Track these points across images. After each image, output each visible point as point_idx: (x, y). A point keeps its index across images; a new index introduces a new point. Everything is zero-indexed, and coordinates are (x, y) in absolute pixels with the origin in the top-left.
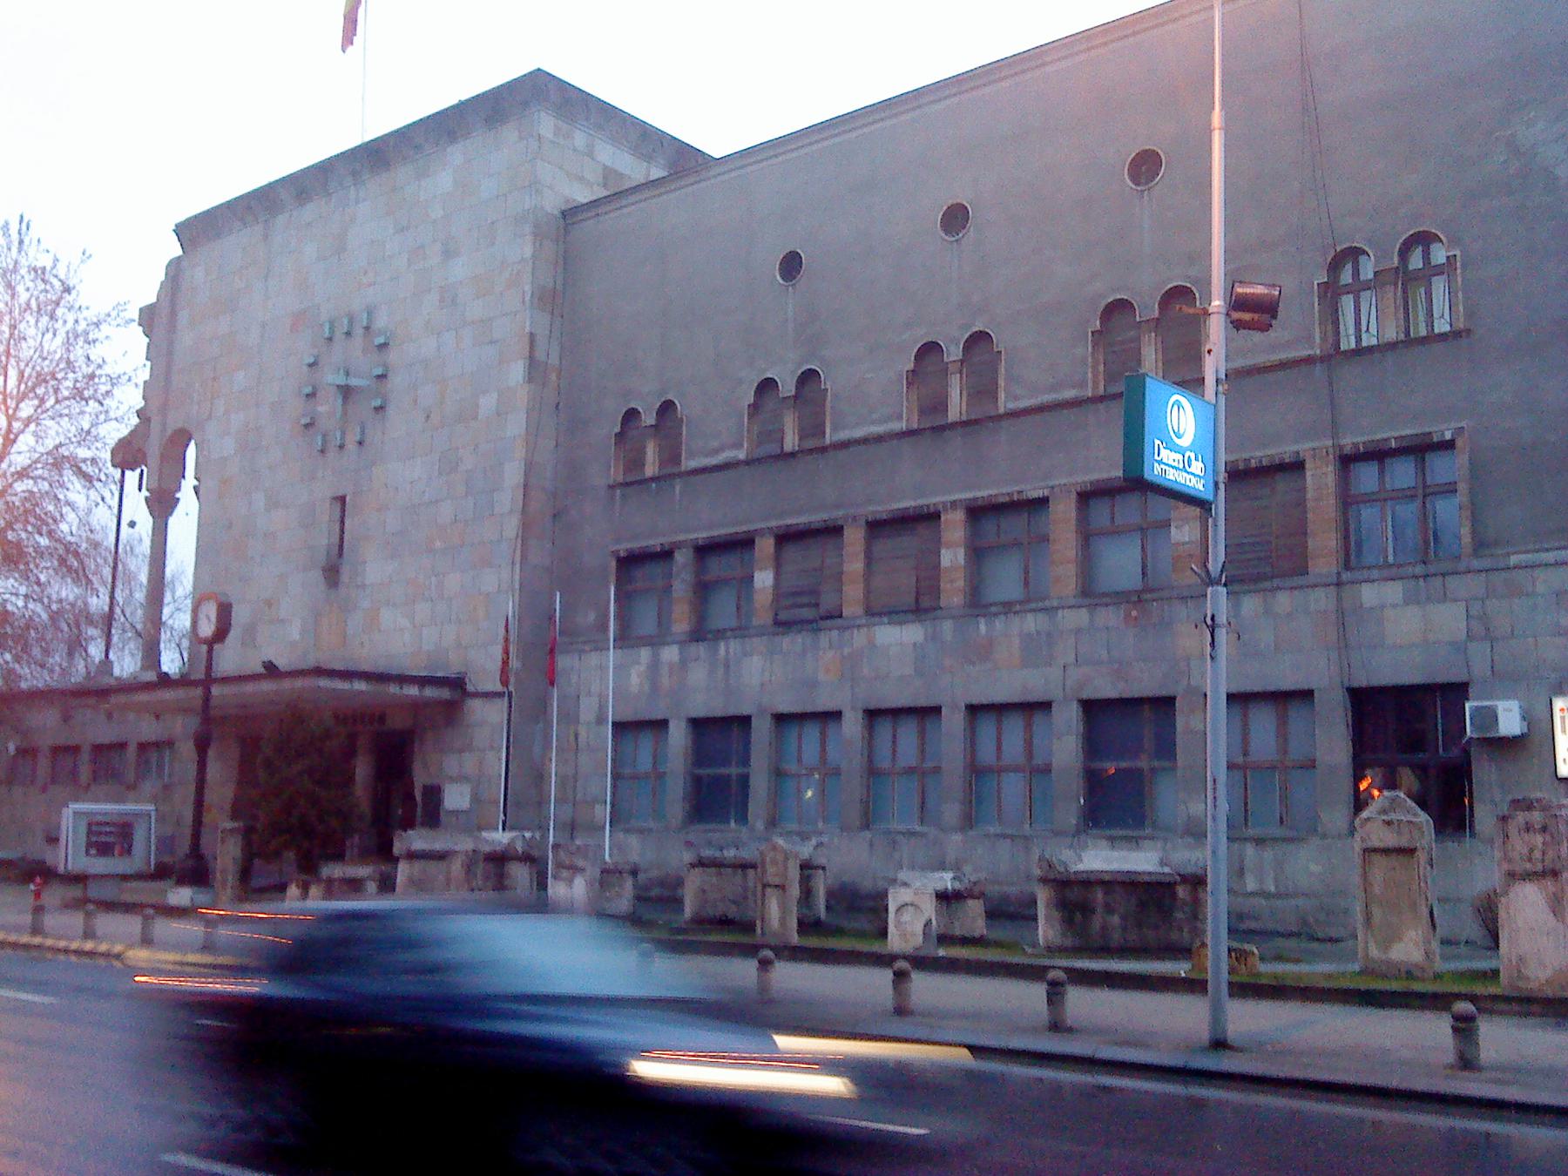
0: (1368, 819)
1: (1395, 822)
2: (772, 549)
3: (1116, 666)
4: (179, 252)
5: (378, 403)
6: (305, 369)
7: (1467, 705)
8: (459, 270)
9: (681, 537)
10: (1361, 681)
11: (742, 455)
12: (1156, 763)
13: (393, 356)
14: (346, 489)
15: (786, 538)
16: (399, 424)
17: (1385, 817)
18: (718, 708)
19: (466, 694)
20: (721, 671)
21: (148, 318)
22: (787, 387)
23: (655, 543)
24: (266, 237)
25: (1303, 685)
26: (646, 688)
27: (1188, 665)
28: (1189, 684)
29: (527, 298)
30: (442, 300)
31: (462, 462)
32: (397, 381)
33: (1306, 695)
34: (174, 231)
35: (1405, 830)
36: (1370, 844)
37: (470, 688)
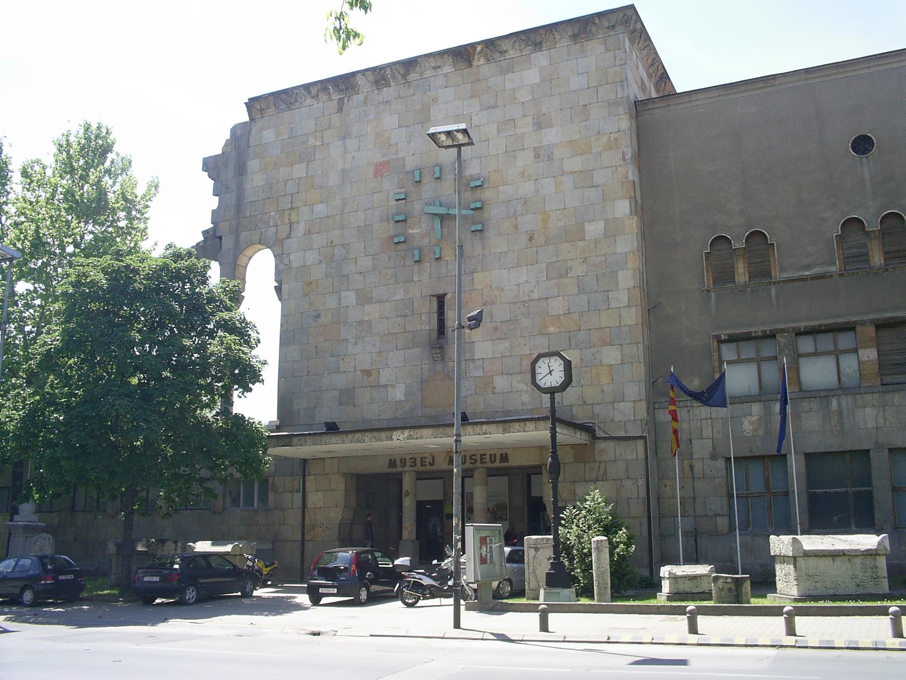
2: (873, 335)
4: (248, 119)
5: (479, 227)
6: (393, 203)
8: (551, 136)
9: (782, 326)
11: (833, 269)
13: (488, 195)
14: (449, 289)
15: (881, 326)
16: (497, 243)
18: (831, 443)
19: (594, 437)
20: (835, 420)
21: (211, 166)
22: (872, 225)
23: (758, 330)
24: (340, 109)
26: (761, 432)
29: (628, 156)
30: (537, 156)
31: (571, 270)
32: (494, 213)
34: (246, 103)
37: (599, 434)
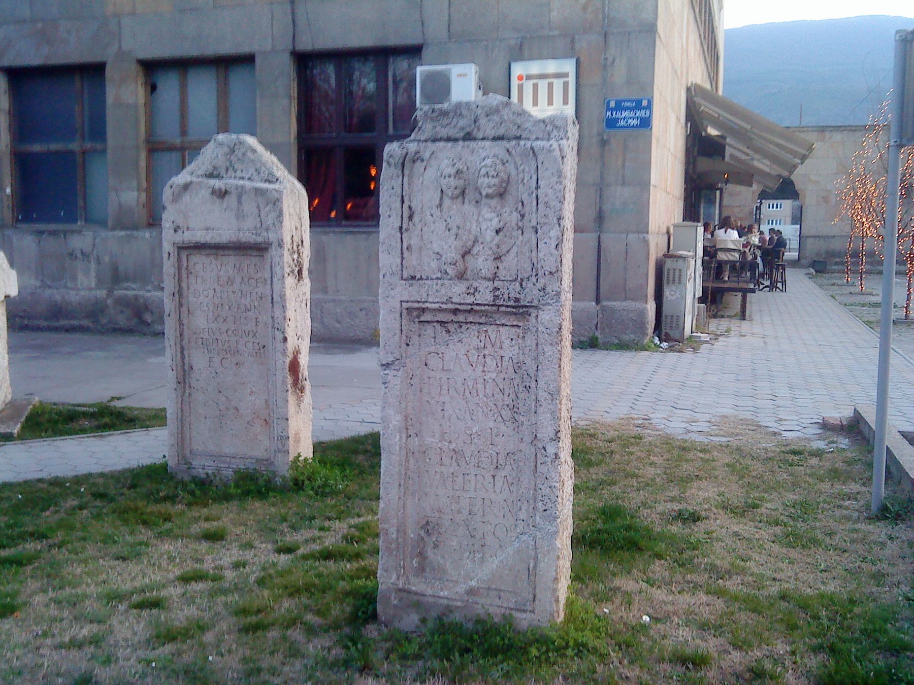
0: (186, 187)
1: (233, 190)
3: (40, 25)
7: (419, 70)
10: (306, 44)
12: (88, 145)
17: (217, 184)
25: (245, 49)
27: (119, 24)
28: (120, 47)
33: (248, 60)
35: (249, 206)
36: (188, 237)
